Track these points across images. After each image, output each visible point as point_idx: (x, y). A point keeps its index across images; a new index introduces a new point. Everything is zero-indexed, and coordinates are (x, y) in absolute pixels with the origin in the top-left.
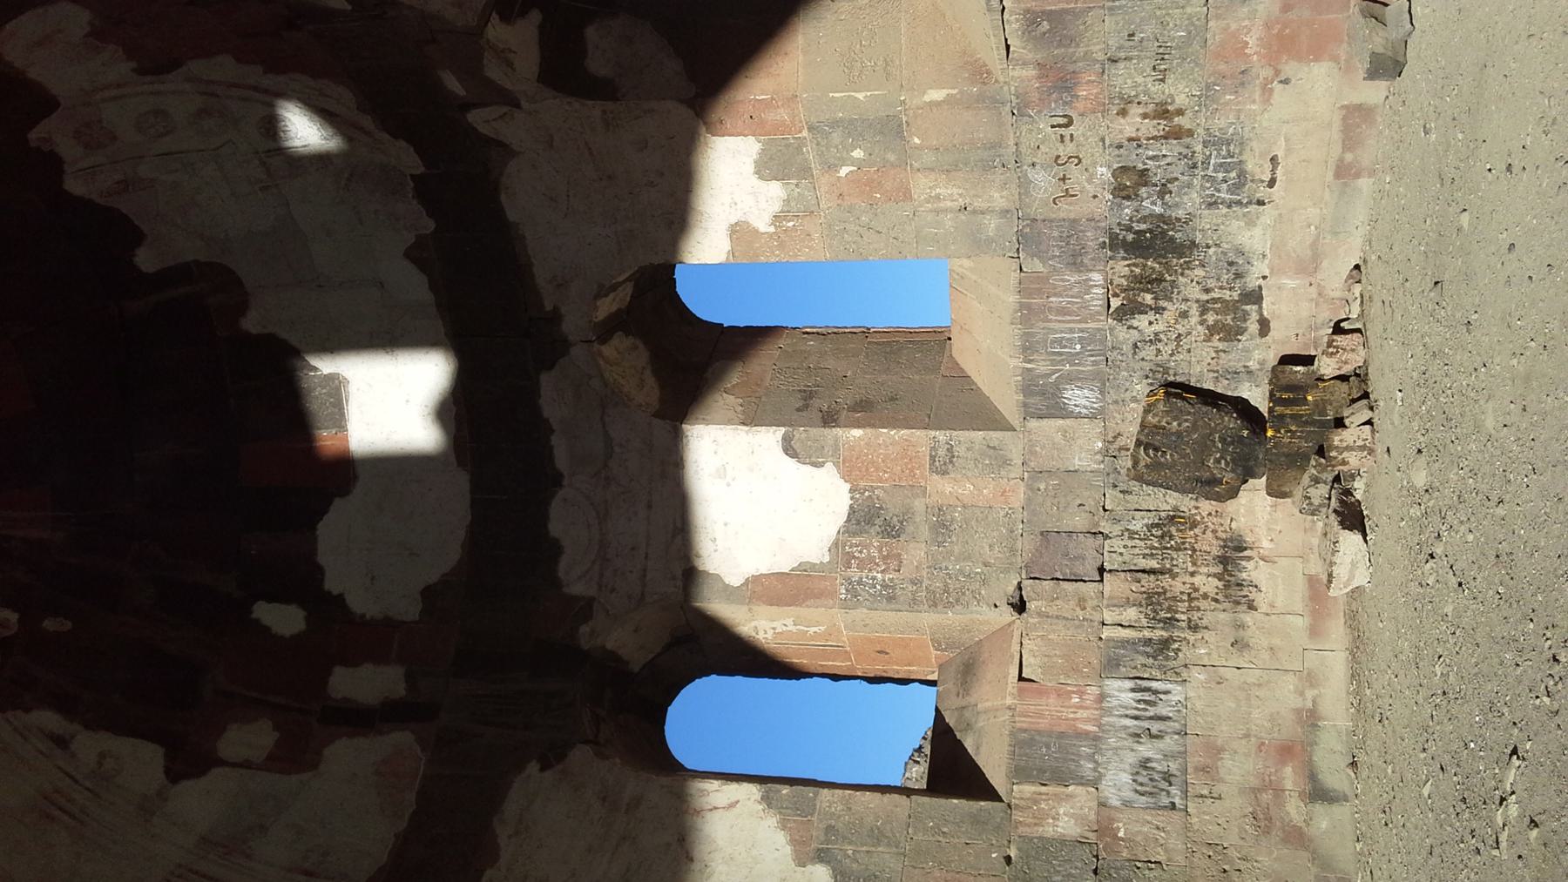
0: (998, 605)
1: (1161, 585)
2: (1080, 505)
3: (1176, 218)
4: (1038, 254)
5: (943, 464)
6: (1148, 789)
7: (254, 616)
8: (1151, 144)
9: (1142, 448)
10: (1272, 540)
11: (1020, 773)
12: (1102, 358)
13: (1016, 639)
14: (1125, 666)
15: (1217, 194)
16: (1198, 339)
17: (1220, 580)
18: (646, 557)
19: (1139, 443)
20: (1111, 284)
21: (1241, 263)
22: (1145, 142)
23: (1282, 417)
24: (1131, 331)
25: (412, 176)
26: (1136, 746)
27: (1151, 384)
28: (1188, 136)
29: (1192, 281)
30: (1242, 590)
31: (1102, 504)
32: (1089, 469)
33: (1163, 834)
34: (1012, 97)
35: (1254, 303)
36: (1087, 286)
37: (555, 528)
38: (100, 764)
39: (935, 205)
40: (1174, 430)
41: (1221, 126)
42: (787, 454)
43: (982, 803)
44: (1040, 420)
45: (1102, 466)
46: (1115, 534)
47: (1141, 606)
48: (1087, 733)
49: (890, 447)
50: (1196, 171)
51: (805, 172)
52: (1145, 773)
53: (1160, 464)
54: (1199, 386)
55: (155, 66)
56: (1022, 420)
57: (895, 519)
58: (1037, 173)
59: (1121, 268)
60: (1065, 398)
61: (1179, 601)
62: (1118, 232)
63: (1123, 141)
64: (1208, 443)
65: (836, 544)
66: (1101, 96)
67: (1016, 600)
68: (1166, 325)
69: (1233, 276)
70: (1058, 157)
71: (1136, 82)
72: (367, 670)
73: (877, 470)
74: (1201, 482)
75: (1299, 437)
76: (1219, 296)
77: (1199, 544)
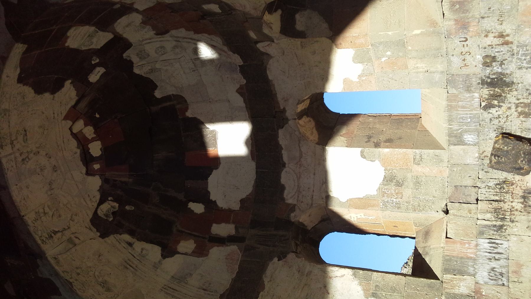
0: (438, 211)
1: (500, 206)
2: (470, 176)
3: (506, 73)
4: (455, 87)
5: (418, 161)
6: (494, 278)
7: (189, 207)
8: (497, 47)
9: (493, 156)
11: (446, 271)
13: (445, 224)
14: (485, 234)
16: (515, 117)
17: (522, 204)
18: (313, 191)
19: (492, 154)
20: (482, 97)
22: (495, 46)
24: (489, 114)
25: (239, 66)
26: (490, 263)
27: (497, 133)
29: (512, 96)
31: (478, 176)
33: (499, 294)
34: (445, 31)
36: (473, 98)
37: (283, 181)
39: (416, 70)
40: (506, 150)
42: (362, 157)
43: (432, 280)
44: (455, 146)
45: (478, 163)
46: (482, 187)
47: (492, 213)
48: (471, 258)
49: (399, 155)
50: (514, 56)
51: (370, 60)
52: (493, 272)
54: (515, 134)
55: (161, 32)
56: (448, 146)
57: (400, 180)
58: (454, 58)
59: (486, 92)
60: (464, 138)
61: (507, 212)
62: (484, 78)
64: (519, 154)
66: (478, 30)
67: (445, 210)
68: (502, 112)
70: (462, 52)
71: (491, 25)
72: (223, 225)
74: (516, 169)
76: (522, 101)
77: (515, 191)
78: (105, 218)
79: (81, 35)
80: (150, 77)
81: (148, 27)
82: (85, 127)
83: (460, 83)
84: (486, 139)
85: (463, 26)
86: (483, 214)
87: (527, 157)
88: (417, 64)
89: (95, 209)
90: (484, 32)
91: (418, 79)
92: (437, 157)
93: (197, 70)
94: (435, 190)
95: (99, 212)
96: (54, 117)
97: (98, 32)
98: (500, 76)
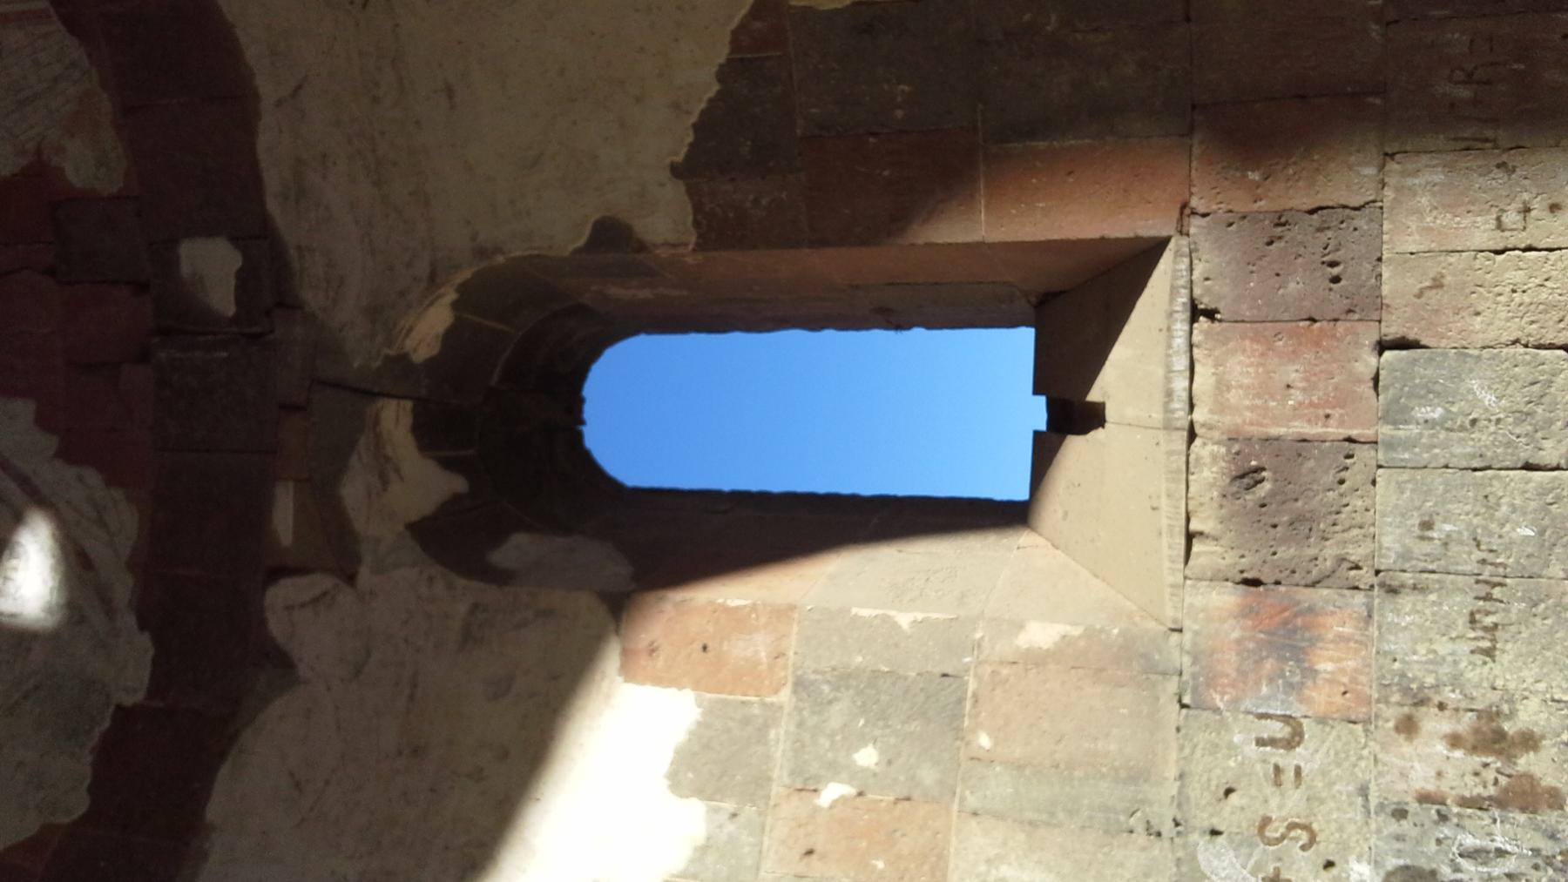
8: (1470, 817)
22: (1456, 810)
25: (119, 708)
28: (1551, 807)
51: (756, 787)
58: (1218, 856)
63: (1409, 799)
70: (1266, 821)
71: (1435, 652)
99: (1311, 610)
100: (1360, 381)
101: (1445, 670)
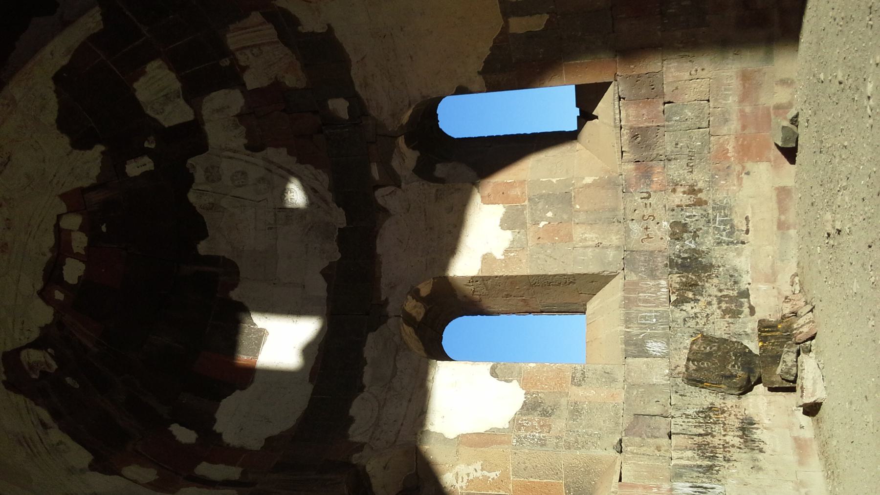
2: (657, 401)
4: (634, 270)
7: (170, 429)
9: (691, 362)
10: (769, 420)
12: (667, 326)
15: (721, 238)
17: (741, 438)
18: (402, 425)
19: (688, 360)
20: (671, 287)
21: (736, 275)
22: (685, 208)
23: (766, 337)
24: (682, 312)
25: (339, 228)
29: (712, 285)
30: (755, 443)
32: (661, 383)
34: (623, 181)
35: (745, 298)
36: (658, 287)
37: (352, 412)
38: (58, 444)
39: (584, 244)
40: (708, 351)
41: (720, 199)
42: (492, 376)
44: (634, 358)
45: (669, 382)
47: (695, 450)
50: (710, 225)
51: (523, 225)
53: (703, 368)
55: (254, 146)
56: (624, 358)
57: (549, 408)
58: (634, 225)
62: (673, 258)
63: (675, 207)
64: (727, 357)
65: (513, 420)
66: (664, 181)
69: (733, 283)
70: (644, 216)
73: (542, 383)
74: (725, 377)
75: (776, 345)
76: (727, 293)
78: (27, 368)
79: (158, 86)
80: (205, 216)
81: (242, 128)
82: (78, 230)
83: (642, 264)
84: (679, 349)
85: (646, 174)
86: (680, 452)
87: (740, 359)
88: (585, 233)
89: (19, 346)
90: (671, 184)
91: (586, 258)
92: (607, 374)
93: (276, 228)
94: (604, 421)
95: (24, 353)
96: (52, 180)
97: (179, 97)
98: (693, 255)
99: (651, 167)
100: (660, 112)
101: (682, 177)
